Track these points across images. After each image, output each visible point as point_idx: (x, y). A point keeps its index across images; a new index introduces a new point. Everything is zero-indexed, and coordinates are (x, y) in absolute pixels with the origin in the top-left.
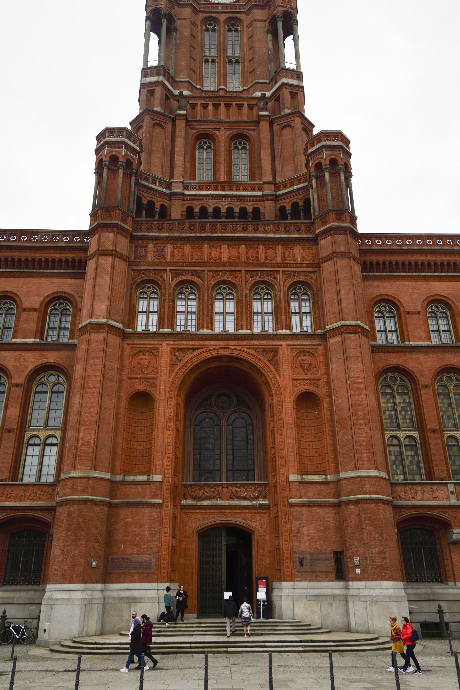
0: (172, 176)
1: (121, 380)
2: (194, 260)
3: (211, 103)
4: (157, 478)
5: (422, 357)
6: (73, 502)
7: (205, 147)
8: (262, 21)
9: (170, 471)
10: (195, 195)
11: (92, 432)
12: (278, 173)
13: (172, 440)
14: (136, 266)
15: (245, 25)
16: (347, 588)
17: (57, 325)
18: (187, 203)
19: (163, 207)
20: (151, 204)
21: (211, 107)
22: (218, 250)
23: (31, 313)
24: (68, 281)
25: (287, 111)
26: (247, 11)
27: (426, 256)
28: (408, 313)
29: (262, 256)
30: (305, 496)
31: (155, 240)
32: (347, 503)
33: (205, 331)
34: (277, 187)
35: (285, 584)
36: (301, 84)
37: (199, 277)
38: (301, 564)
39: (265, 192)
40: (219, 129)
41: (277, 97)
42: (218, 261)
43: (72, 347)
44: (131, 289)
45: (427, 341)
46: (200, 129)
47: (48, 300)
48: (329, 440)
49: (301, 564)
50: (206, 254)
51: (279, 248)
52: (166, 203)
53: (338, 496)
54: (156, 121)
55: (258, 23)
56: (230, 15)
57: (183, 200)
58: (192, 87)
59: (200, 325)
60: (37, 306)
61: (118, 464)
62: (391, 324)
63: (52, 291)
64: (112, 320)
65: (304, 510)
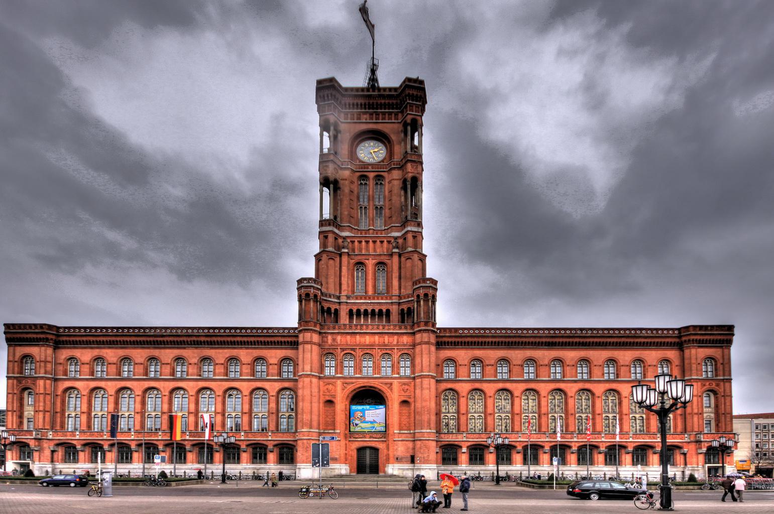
0: (340, 293)
1: (319, 396)
3: (363, 241)
4: (338, 431)
5: (464, 385)
6: (304, 439)
7: (360, 270)
8: (398, 179)
9: (343, 429)
10: (354, 303)
11: (309, 416)
12: (402, 287)
13: (344, 419)
15: (387, 181)
16: (414, 466)
17: (286, 370)
18: (349, 307)
19: (336, 310)
20: (329, 309)
21: (363, 243)
23: (274, 366)
24: (290, 351)
25: (410, 249)
26: (389, 170)
28: (460, 365)
30: (401, 438)
32: (417, 440)
33: (358, 376)
34: (400, 297)
35: (390, 465)
36: (420, 230)
38: (397, 459)
39: (394, 301)
40: (368, 259)
41: (404, 237)
43: (296, 381)
48: (413, 419)
49: (397, 459)
52: (338, 307)
53: (414, 437)
54: (330, 257)
55: (395, 181)
56: (376, 174)
57: (347, 305)
58: (351, 229)
59: (355, 373)
60: (276, 363)
61: (321, 426)
62: (452, 369)
63: (282, 356)
65: (400, 442)
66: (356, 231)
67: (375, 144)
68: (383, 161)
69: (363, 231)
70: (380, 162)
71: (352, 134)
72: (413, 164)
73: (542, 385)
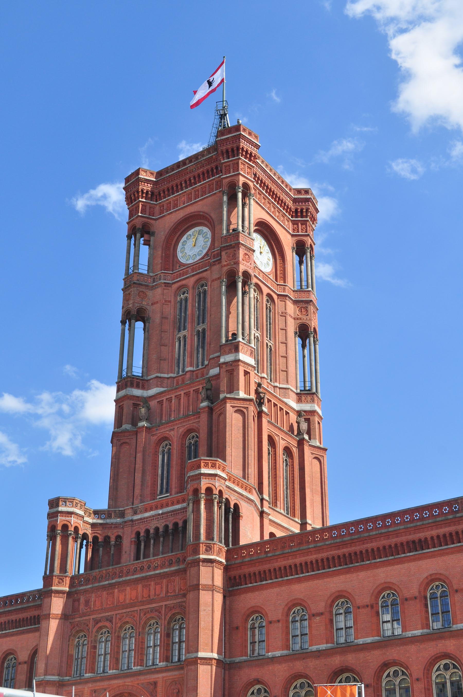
2: (108, 606)
14: (72, 619)
18: (136, 529)
22: (123, 593)
27: (288, 559)
29: (152, 593)
31: (85, 592)
37: (111, 621)
42: (123, 603)
44: (69, 641)
45: (283, 650)
46: (160, 434)
47: (33, 652)
50: (116, 598)
51: (165, 581)
64: (49, 675)
73: (412, 648)
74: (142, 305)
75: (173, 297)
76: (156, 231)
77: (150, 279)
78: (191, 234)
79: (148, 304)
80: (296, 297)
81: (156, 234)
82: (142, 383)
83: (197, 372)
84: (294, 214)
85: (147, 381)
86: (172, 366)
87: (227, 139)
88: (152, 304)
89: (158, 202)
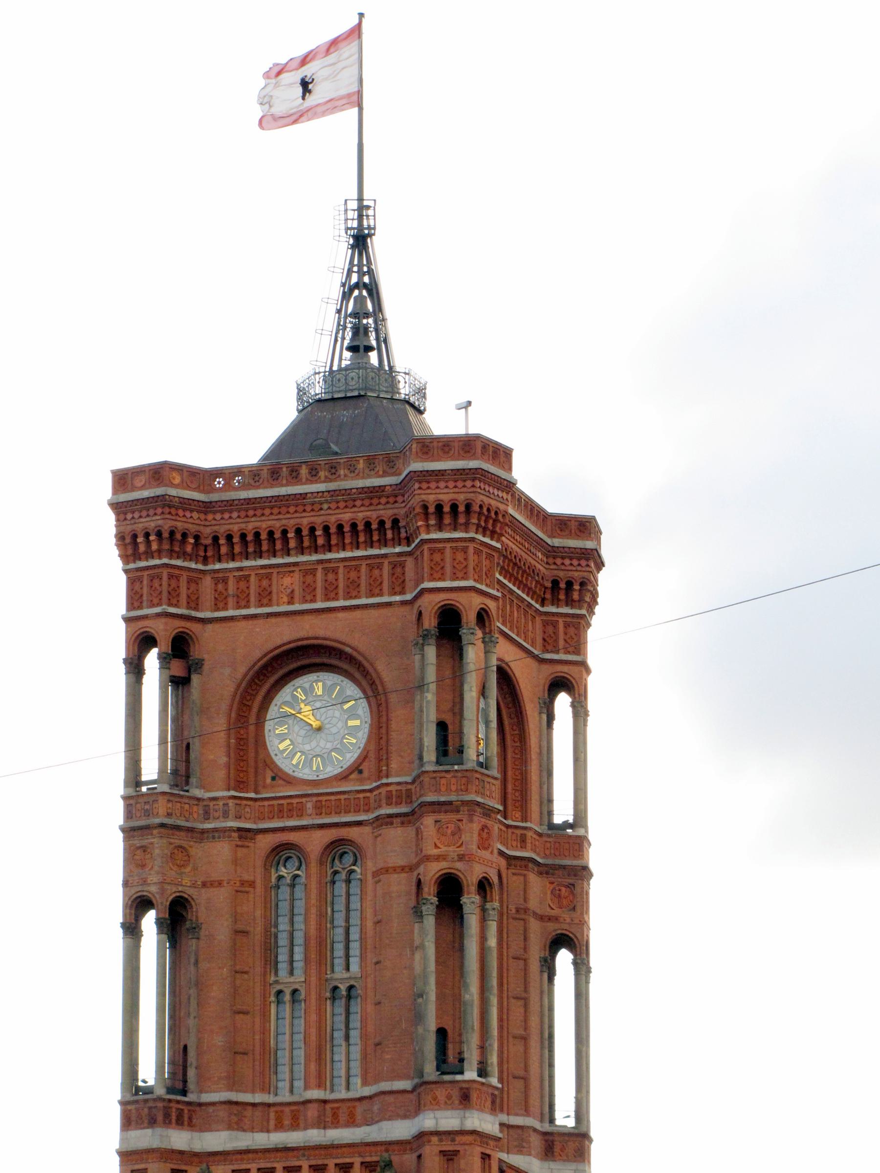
8: (403, 869)
66: (258, 1113)
67: (328, 690)
68: (356, 769)
69: (287, 1110)
70: (344, 777)
71: (242, 670)
72: (442, 817)
74: (180, 889)
75: (259, 871)
76: (206, 656)
77: (195, 808)
78: (307, 686)
79: (194, 886)
80: (547, 852)
81: (206, 668)
82: (189, 1111)
83: (336, 1105)
84: (548, 596)
85: (200, 1105)
86: (262, 1073)
87: (440, 473)
88: (204, 884)
89: (210, 567)
